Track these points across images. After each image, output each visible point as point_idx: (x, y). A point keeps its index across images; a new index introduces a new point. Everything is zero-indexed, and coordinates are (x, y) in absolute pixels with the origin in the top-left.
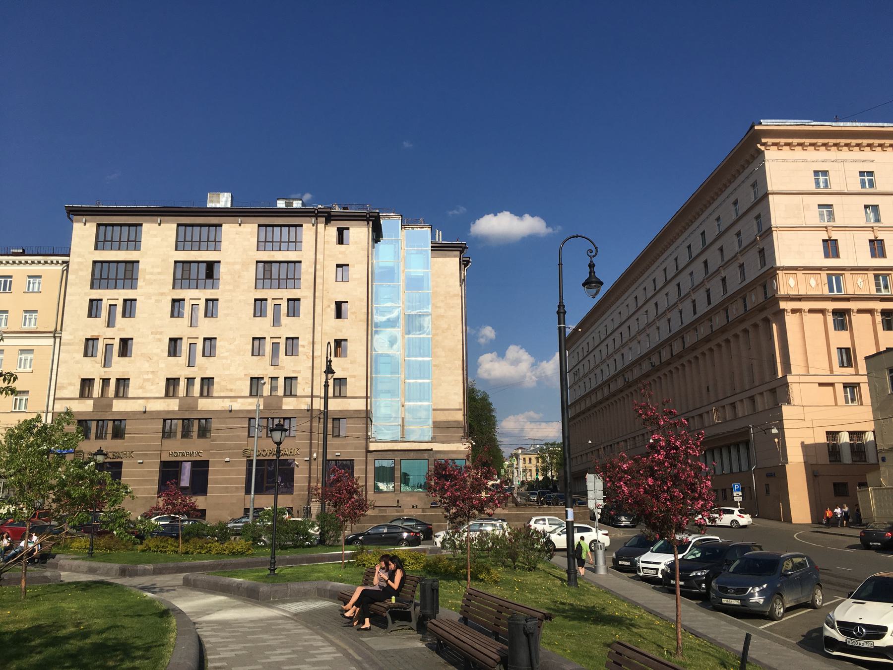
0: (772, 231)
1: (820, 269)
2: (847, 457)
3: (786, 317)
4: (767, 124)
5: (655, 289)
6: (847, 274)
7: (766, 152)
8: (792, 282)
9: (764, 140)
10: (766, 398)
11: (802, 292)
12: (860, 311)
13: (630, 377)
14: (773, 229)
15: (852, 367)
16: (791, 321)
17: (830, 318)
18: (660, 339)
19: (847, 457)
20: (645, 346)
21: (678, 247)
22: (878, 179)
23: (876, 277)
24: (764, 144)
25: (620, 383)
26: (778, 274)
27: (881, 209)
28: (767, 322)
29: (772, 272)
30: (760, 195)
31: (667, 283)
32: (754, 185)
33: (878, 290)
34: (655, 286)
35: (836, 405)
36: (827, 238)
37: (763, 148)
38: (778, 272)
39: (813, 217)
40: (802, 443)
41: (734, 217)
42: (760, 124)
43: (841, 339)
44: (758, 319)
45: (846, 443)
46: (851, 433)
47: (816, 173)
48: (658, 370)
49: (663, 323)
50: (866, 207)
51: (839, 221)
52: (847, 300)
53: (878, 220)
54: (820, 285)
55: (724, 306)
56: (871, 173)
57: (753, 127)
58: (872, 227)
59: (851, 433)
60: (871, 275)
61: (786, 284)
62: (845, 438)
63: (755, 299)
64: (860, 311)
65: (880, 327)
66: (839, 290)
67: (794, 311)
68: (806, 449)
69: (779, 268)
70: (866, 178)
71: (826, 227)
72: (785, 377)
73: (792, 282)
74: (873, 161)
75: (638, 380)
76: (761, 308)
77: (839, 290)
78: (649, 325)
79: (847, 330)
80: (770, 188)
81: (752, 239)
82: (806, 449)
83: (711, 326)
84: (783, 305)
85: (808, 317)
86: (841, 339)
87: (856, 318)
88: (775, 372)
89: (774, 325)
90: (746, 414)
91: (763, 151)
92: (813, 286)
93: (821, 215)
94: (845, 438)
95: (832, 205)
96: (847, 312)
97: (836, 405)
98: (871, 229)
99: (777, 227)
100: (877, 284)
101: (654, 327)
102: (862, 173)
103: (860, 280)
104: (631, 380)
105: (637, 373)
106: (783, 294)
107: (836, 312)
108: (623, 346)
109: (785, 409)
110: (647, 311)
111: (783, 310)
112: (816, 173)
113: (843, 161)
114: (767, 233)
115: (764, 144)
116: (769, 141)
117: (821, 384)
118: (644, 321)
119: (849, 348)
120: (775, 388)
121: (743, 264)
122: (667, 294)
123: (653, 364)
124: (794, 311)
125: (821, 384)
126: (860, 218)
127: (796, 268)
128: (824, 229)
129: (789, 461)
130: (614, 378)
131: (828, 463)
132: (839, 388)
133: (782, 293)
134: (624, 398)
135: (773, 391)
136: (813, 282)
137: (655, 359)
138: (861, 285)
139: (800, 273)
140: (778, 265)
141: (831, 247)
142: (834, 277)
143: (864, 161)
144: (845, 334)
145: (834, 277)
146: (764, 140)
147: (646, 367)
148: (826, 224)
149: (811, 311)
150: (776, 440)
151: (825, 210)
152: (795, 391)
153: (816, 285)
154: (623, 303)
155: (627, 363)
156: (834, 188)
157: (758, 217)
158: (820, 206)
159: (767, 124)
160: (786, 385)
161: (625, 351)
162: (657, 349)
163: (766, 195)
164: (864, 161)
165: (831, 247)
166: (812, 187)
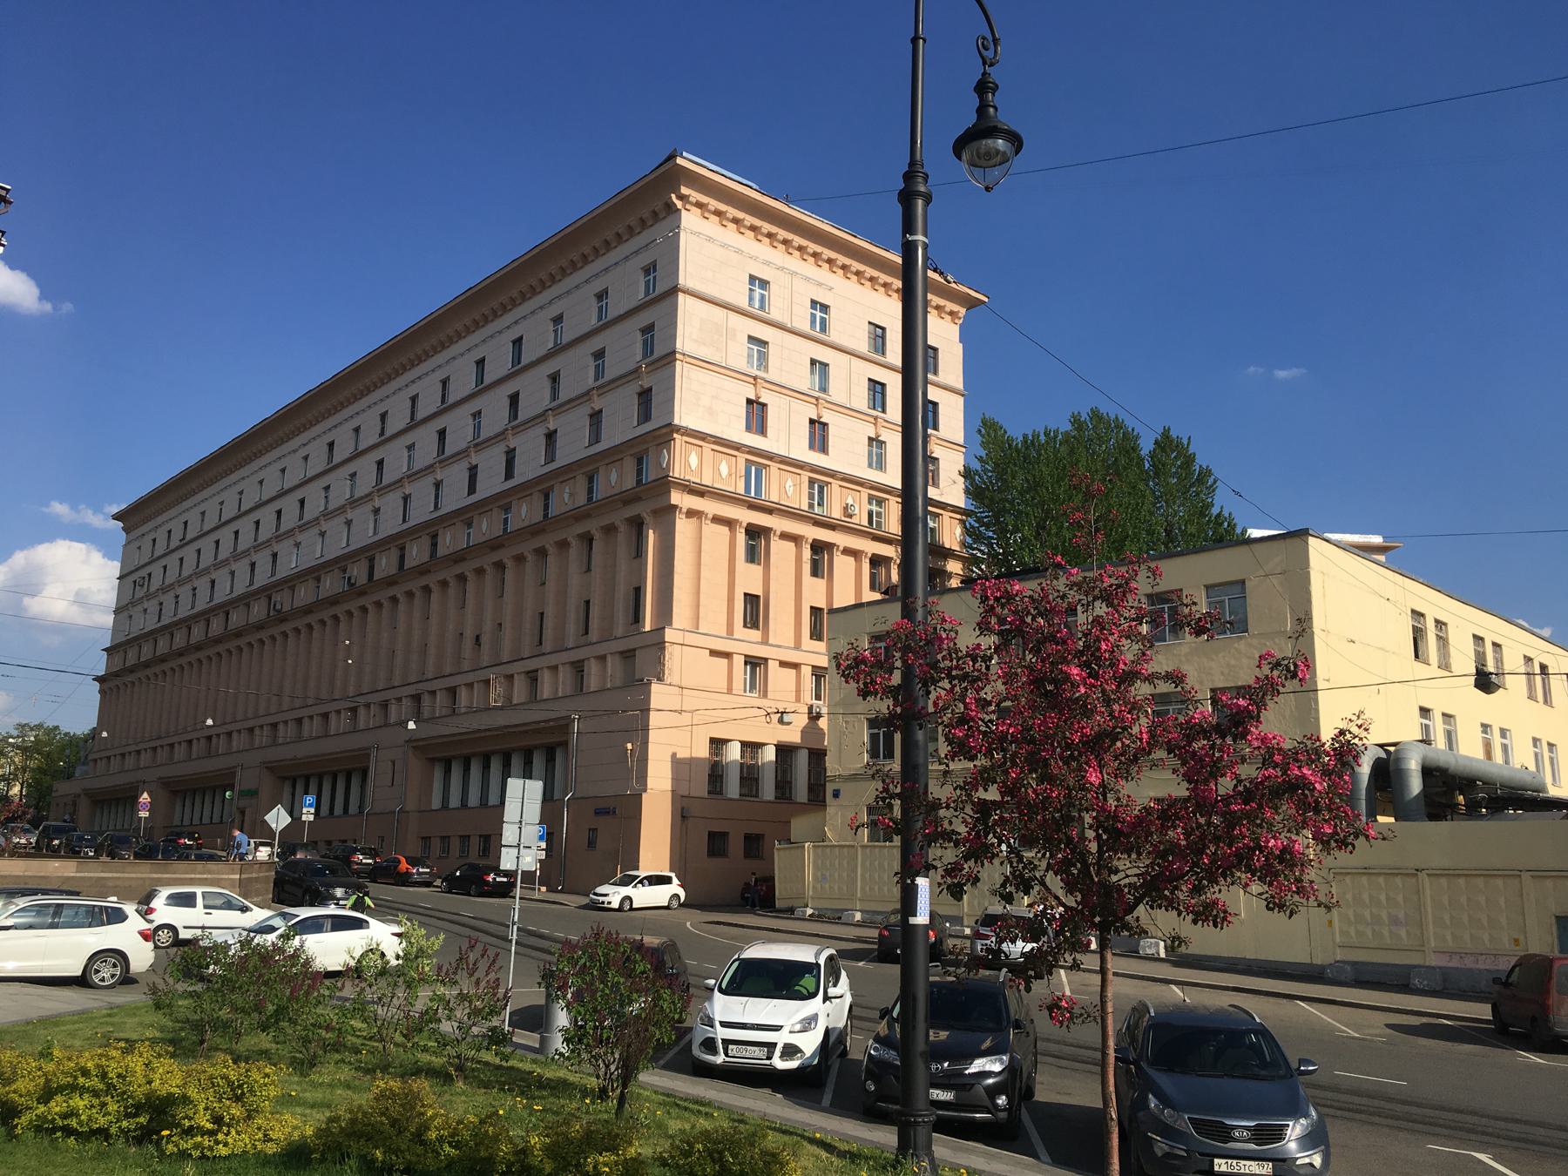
0: (676, 360)
1: (738, 447)
2: (733, 788)
3: (677, 520)
5: (382, 434)
6: (774, 466)
7: (683, 212)
8: (694, 460)
9: (684, 190)
10: (609, 664)
11: (707, 481)
12: (785, 536)
13: (283, 601)
14: (678, 356)
15: (758, 629)
16: (683, 528)
18: (375, 533)
19: (733, 788)
20: (338, 542)
21: (454, 358)
23: (812, 482)
24: (682, 197)
25: (258, 611)
26: (674, 439)
27: (832, 371)
28: (638, 526)
29: (666, 433)
30: (660, 289)
31: (414, 425)
32: (649, 270)
33: (811, 506)
34: (383, 429)
35: (730, 691)
36: (753, 398)
37: (679, 204)
38: (675, 435)
39: (739, 355)
40: (674, 755)
41: (594, 321)
43: (750, 579)
44: (619, 517)
45: (736, 761)
46: (744, 744)
47: (752, 279)
48: (362, 593)
49: (392, 502)
50: (813, 362)
51: (773, 375)
52: (769, 511)
53: (824, 389)
54: (733, 476)
55: (543, 487)
57: (672, 157)
58: (817, 399)
59: (744, 744)
60: (806, 475)
61: (686, 462)
62: (734, 753)
63: (617, 479)
64: (785, 536)
65: (807, 568)
67: (691, 513)
68: (677, 763)
69: (678, 429)
70: (818, 314)
71: (755, 378)
72: (659, 630)
74: (831, 289)
75: (308, 610)
76: (628, 499)
78: (354, 503)
79: (759, 564)
80: (684, 280)
81: (633, 366)
82: (677, 763)
83: (506, 520)
84: (676, 498)
85: (710, 529)
86: (750, 579)
88: (637, 617)
89: (651, 532)
90: (560, 695)
91: (679, 210)
92: (724, 477)
94: (734, 753)
95: (766, 343)
97: (730, 691)
98: (814, 401)
99: (684, 355)
100: (811, 497)
101: (369, 507)
102: (814, 303)
103: (789, 483)
104: (287, 607)
105: (304, 595)
106: (677, 476)
108: (279, 537)
109: (655, 688)
110: (353, 475)
111: (675, 507)
112: (752, 279)
113: (793, 274)
115: (682, 197)
116: (695, 196)
117: (714, 653)
118: (341, 491)
119: (757, 597)
120: (634, 650)
121: (601, 411)
122: (411, 447)
123: (353, 581)
125: (714, 653)
126: (804, 380)
128: (752, 380)
129: (649, 786)
130: (245, 600)
131: (706, 795)
132: (739, 661)
133: (676, 475)
134: (252, 646)
135: (628, 655)
136: (724, 469)
137: (358, 572)
138: (790, 491)
139: (707, 447)
140: (676, 421)
141: (757, 414)
142: (753, 468)
143: (820, 284)
144: (756, 570)
145: (753, 468)
146: (684, 190)
147: (331, 585)
148: (755, 372)
149: (717, 520)
150: (629, 746)
151: (755, 348)
153: (725, 473)
154: (294, 451)
155: (282, 573)
156: (775, 314)
157: (648, 330)
158: (751, 339)
160: (660, 645)
161: (284, 548)
162: (368, 553)
163: (674, 290)
164: (820, 284)
165: (757, 414)
166: (743, 302)
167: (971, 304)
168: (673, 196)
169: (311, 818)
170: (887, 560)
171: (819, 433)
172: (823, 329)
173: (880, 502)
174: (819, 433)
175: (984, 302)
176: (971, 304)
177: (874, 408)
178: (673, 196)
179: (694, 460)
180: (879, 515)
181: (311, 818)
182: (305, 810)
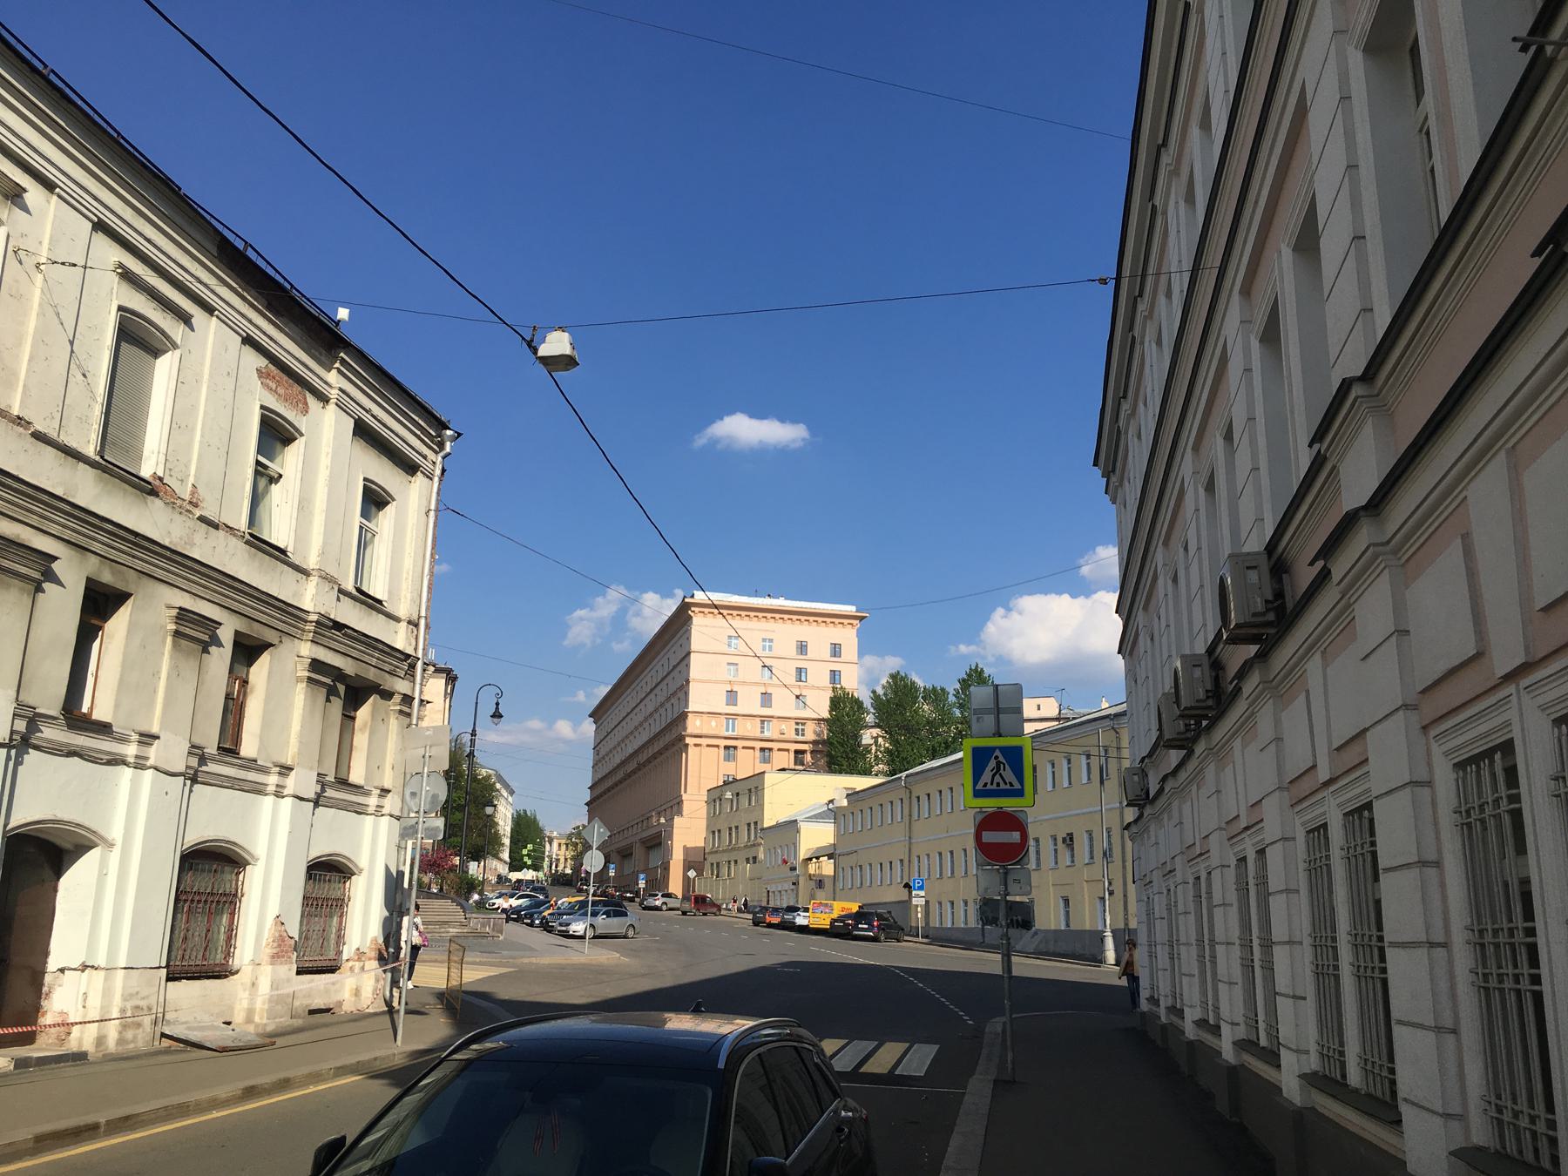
4: (700, 596)
7: (694, 619)
9: (693, 609)
11: (705, 732)
16: (691, 750)
17: (722, 750)
22: (773, 645)
23: (762, 722)
24: (693, 612)
29: (683, 717)
33: (762, 732)
36: (729, 689)
37: (692, 614)
40: (684, 847)
42: (693, 596)
51: (741, 678)
52: (736, 739)
56: (771, 640)
57: (684, 600)
60: (758, 720)
61: (694, 725)
65: (758, 760)
66: (733, 731)
67: (696, 745)
70: (768, 644)
73: (698, 723)
77: (733, 731)
82: (686, 849)
84: (688, 740)
87: (740, 752)
93: (729, 670)
96: (735, 748)
100: (762, 728)
102: (764, 640)
107: (727, 748)
111: (688, 744)
114: (688, 682)
115: (693, 612)
116: (697, 610)
124: (696, 745)
127: (702, 713)
136: (713, 724)
141: (732, 696)
148: (731, 678)
152: (687, 807)
153: (714, 726)
158: (729, 664)
159: (700, 596)
163: (689, 654)
165: (732, 696)
167: (861, 619)
168: (690, 612)
169: (644, 886)
170: (803, 752)
171: (766, 698)
172: (770, 648)
173: (803, 724)
174: (766, 698)
175: (866, 617)
176: (861, 619)
177: (801, 681)
178: (690, 612)
179: (698, 723)
180: (803, 730)
181: (644, 886)
182: (640, 882)
